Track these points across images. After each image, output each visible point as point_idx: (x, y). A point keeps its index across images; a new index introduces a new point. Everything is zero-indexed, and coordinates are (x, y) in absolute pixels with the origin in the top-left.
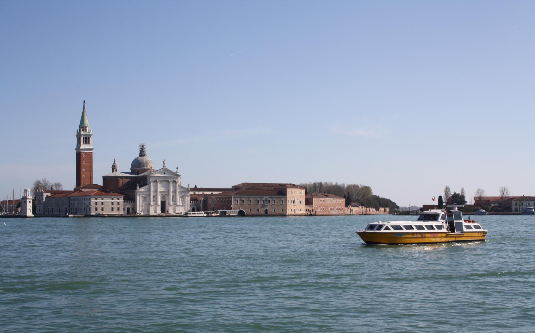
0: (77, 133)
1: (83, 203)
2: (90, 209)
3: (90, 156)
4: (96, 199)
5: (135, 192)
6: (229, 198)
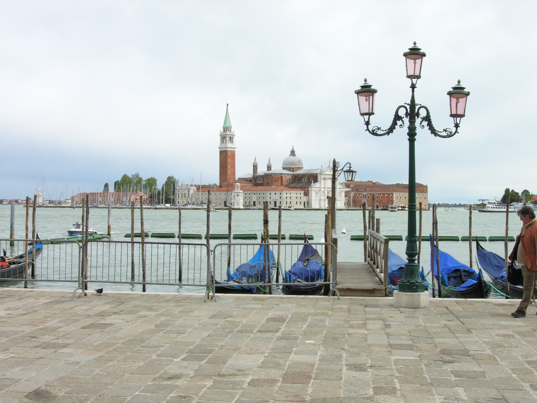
0: (221, 132)
1: (268, 198)
3: (233, 154)
4: (287, 194)
5: (308, 188)
6: (389, 195)
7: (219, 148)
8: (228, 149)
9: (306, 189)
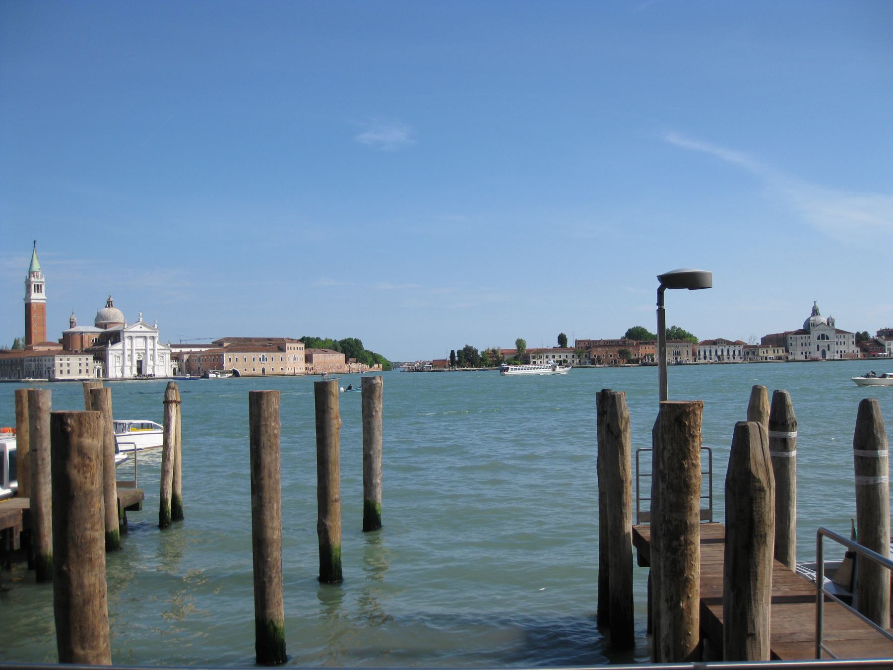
0: (26, 279)
2: (53, 372)
4: (61, 360)
5: (105, 350)
6: (219, 356)
7: (24, 299)
8: (32, 301)
9: (104, 352)
